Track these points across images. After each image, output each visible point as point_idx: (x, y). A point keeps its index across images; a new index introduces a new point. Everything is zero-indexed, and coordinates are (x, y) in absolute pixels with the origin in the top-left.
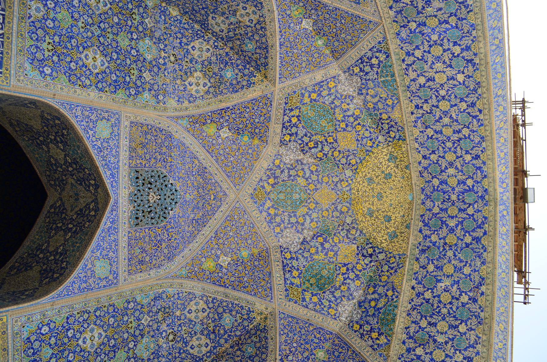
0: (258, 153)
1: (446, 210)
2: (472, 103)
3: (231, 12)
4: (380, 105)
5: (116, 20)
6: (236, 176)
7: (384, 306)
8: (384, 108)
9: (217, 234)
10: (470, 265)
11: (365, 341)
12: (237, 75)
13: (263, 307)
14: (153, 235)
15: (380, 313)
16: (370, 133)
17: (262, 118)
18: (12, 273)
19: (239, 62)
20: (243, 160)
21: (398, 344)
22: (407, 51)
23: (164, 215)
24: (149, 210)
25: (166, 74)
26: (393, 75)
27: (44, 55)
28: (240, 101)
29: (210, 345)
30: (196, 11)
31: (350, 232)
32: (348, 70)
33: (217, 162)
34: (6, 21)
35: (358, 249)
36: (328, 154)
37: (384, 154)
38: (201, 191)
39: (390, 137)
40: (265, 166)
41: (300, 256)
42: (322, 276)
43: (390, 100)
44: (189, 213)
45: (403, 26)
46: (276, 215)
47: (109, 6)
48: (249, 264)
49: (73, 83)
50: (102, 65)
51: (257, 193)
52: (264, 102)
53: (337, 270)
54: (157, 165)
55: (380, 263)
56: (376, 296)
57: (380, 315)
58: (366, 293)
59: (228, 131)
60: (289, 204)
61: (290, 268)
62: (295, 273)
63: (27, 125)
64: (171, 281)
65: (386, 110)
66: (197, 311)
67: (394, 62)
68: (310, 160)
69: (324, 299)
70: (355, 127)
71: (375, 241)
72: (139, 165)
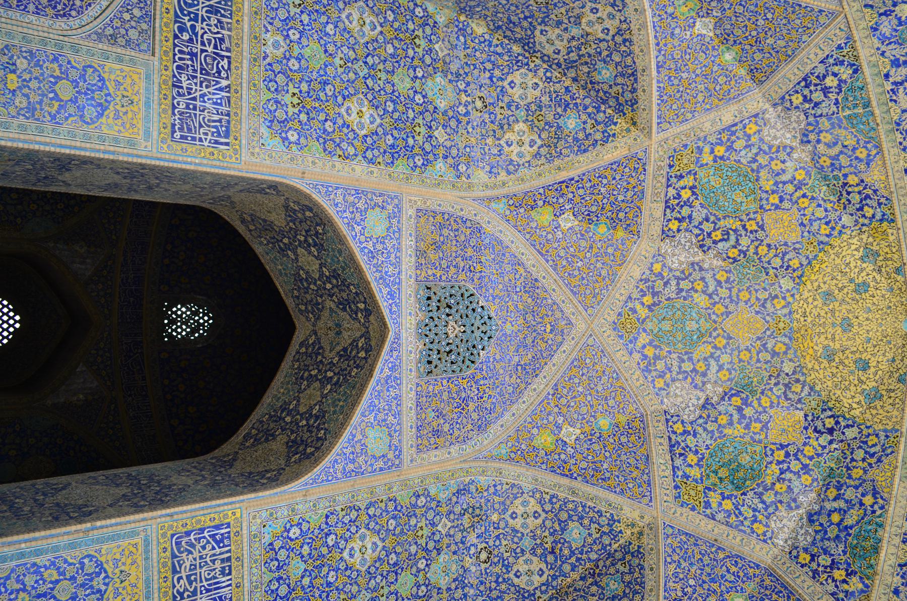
0: (624, 253)
3: (572, 20)
4: (844, 160)
5: (390, 50)
6: (588, 292)
7: (857, 523)
8: (851, 165)
9: (557, 390)
11: (822, 584)
12: (585, 123)
13: (636, 515)
14: (455, 389)
15: (850, 535)
16: (826, 210)
17: (630, 194)
18: (247, 444)
19: (588, 101)
20: (599, 265)
21: (884, 594)
22: (893, 58)
23: (472, 358)
24: (448, 349)
25: (470, 130)
26: (867, 104)
27: (286, 113)
28: (591, 166)
29: (547, 573)
30: (514, 23)
31: (790, 388)
33: (554, 270)
34: (232, 67)
35: (806, 420)
36: (747, 250)
37: (853, 247)
38: (529, 318)
39: (864, 216)
40: (637, 274)
41: (700, 430)
42: (739, 465)
43: (863, 150)
44: (511, 354)
45: (885, 14)
46: (657, 358)
47: (379, 29)
48: (612, 441)
49: (330, 153)
50: (372, 123)
51: (623, 320)
52: (631, 165)
53: (767, 456)
54: (460, 277)
55: (849, 445)
56: (842, 504)
57: (850, 538)
58: (822, 498)
59: (572, 218)
60: (680, 339)
61: (683, 449)
62: (692, 458)
63: (264, 221)
64: (483, 464)
65: (855, 168)
66: (525, 515)
67: (869, 80)
68: (715, 262)
69: (743, 505)
70: (796, 202)
71: (838, 405)
72: (431, 278)
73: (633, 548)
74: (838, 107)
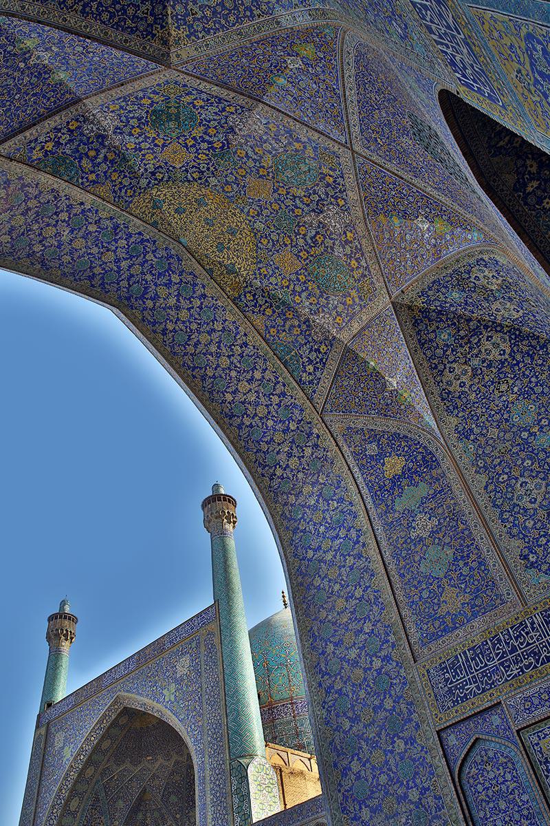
1: (142, 265)
2: (205, 379)
3: (479, 372)
4: (280, 321)
7: (80, 166)
10: (69, 263)
11: (48, 133)
31: (199, 172)
32: (331, 342)
35: (171, 166)
36: (296, 237)
37: (243, 269)
39: (250, 292)
43: (273, 334)
45: (300, 421)
55: (137, 178)
67: (291, 379)
73: (158, 31)
74: (300, 354)
